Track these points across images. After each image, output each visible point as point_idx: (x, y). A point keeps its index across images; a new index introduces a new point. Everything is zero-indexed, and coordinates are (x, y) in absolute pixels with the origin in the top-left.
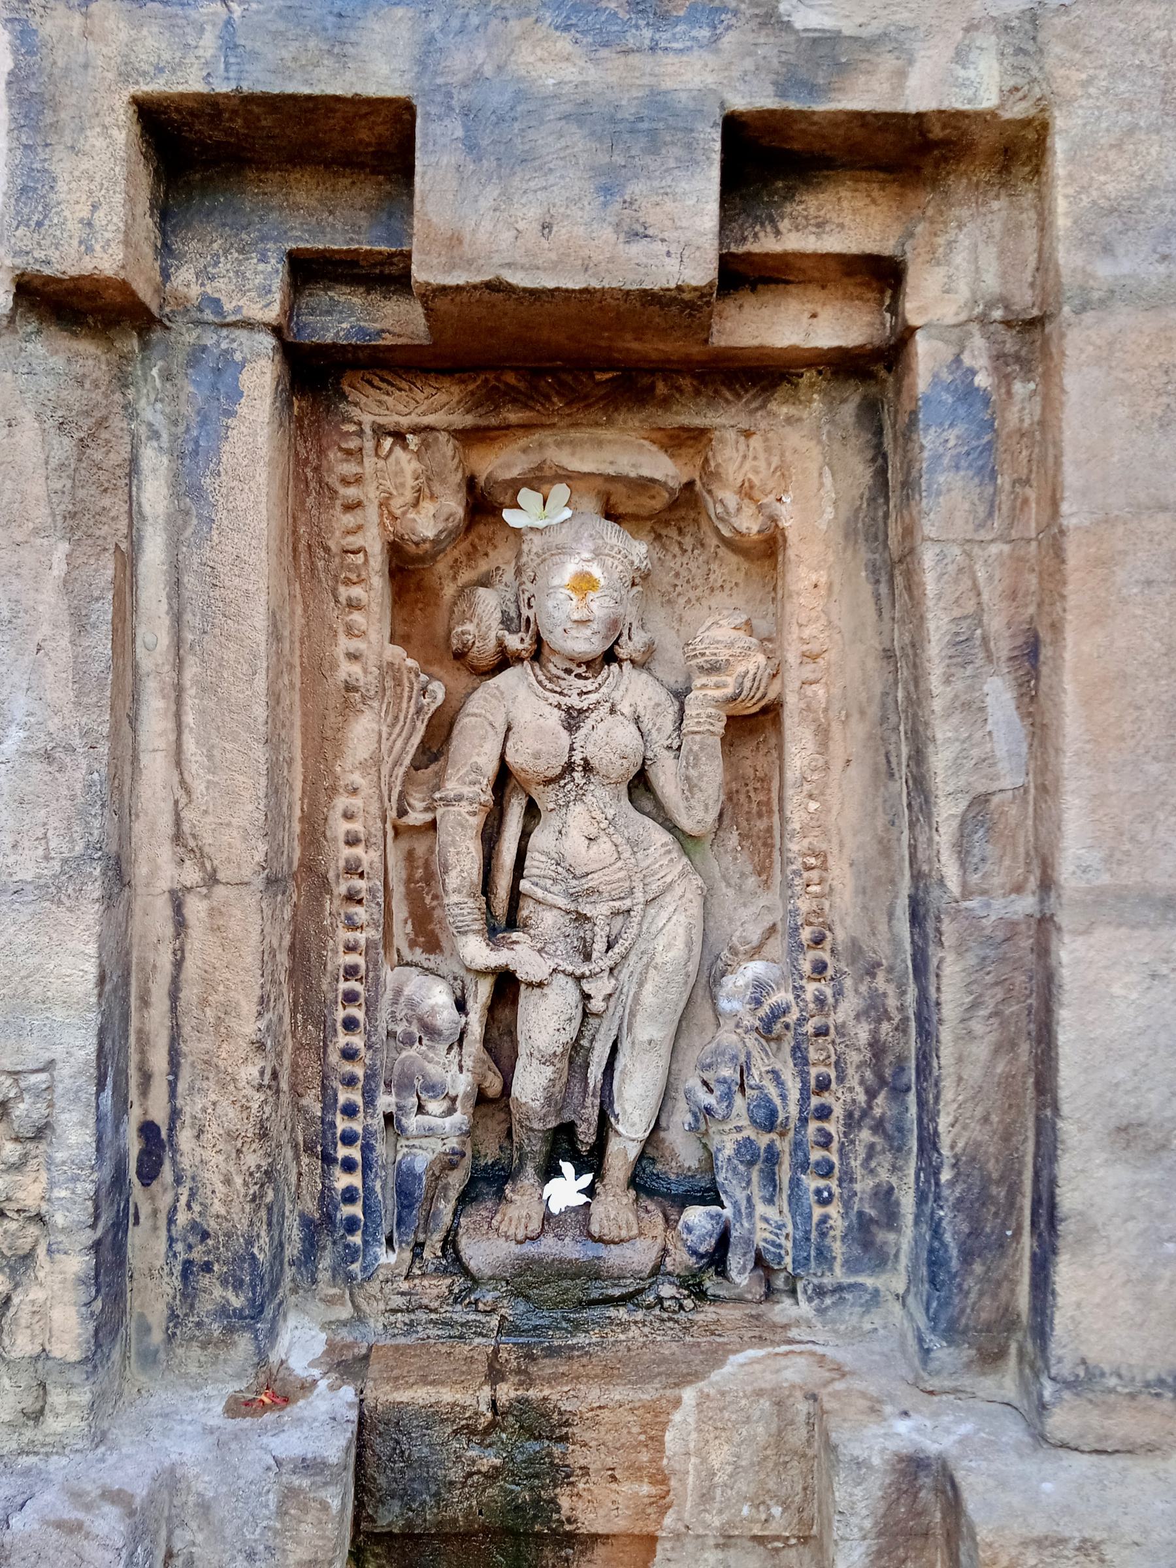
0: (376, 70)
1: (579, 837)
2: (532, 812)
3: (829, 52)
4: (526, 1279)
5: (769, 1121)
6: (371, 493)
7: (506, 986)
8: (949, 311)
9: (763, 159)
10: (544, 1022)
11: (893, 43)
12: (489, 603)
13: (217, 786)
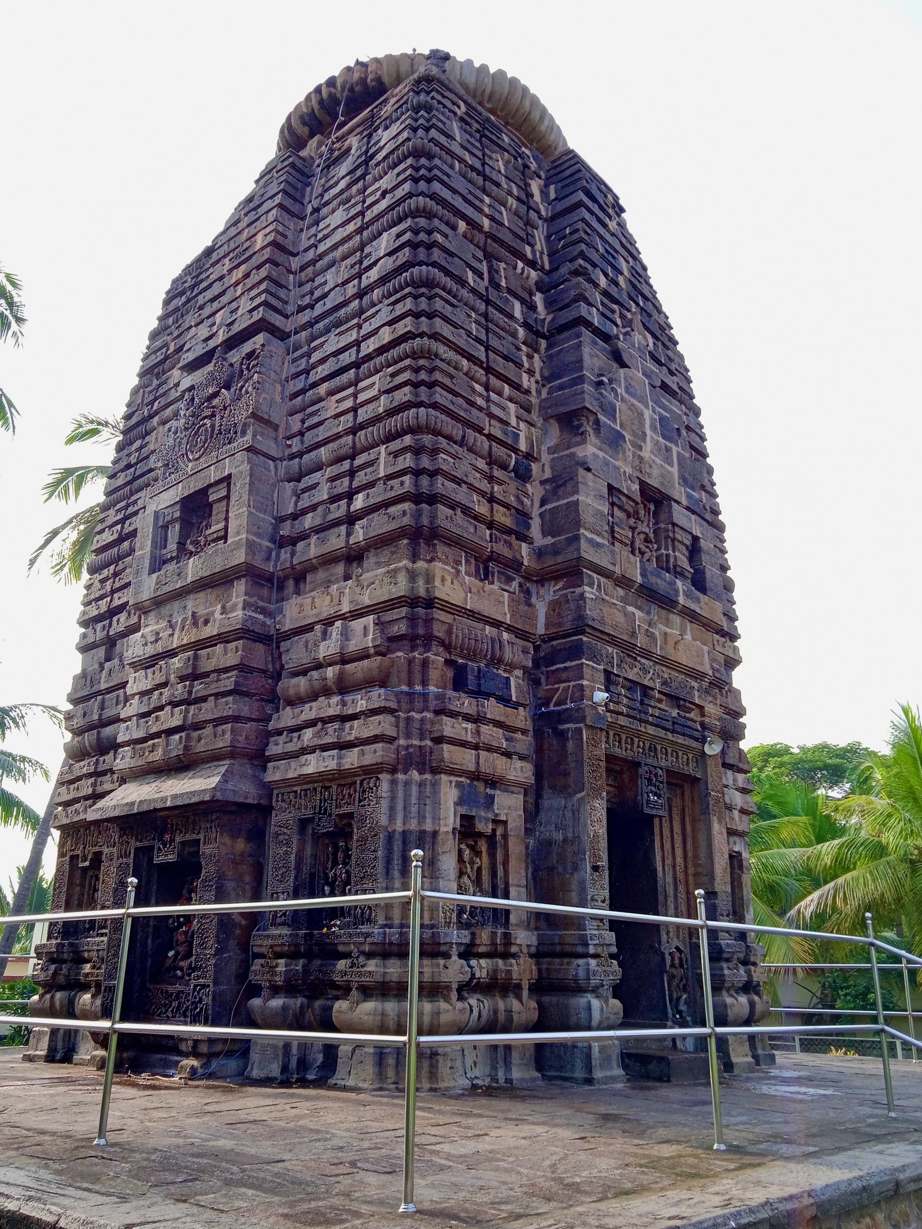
3: (497, 815)
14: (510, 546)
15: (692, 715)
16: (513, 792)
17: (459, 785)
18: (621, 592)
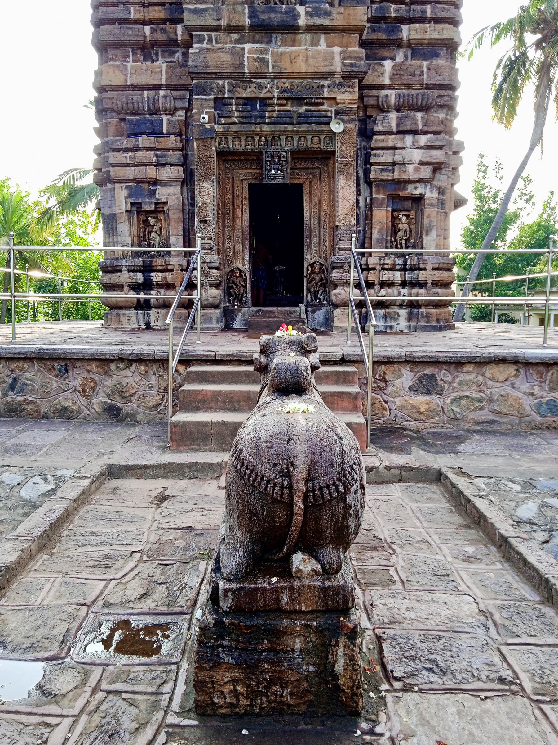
0: (140, 201)
3: (158, 199)
13: (135, 232)
14: (164, 31)
15: (325, 107)
17: (127, 187)
18: (235, 36)
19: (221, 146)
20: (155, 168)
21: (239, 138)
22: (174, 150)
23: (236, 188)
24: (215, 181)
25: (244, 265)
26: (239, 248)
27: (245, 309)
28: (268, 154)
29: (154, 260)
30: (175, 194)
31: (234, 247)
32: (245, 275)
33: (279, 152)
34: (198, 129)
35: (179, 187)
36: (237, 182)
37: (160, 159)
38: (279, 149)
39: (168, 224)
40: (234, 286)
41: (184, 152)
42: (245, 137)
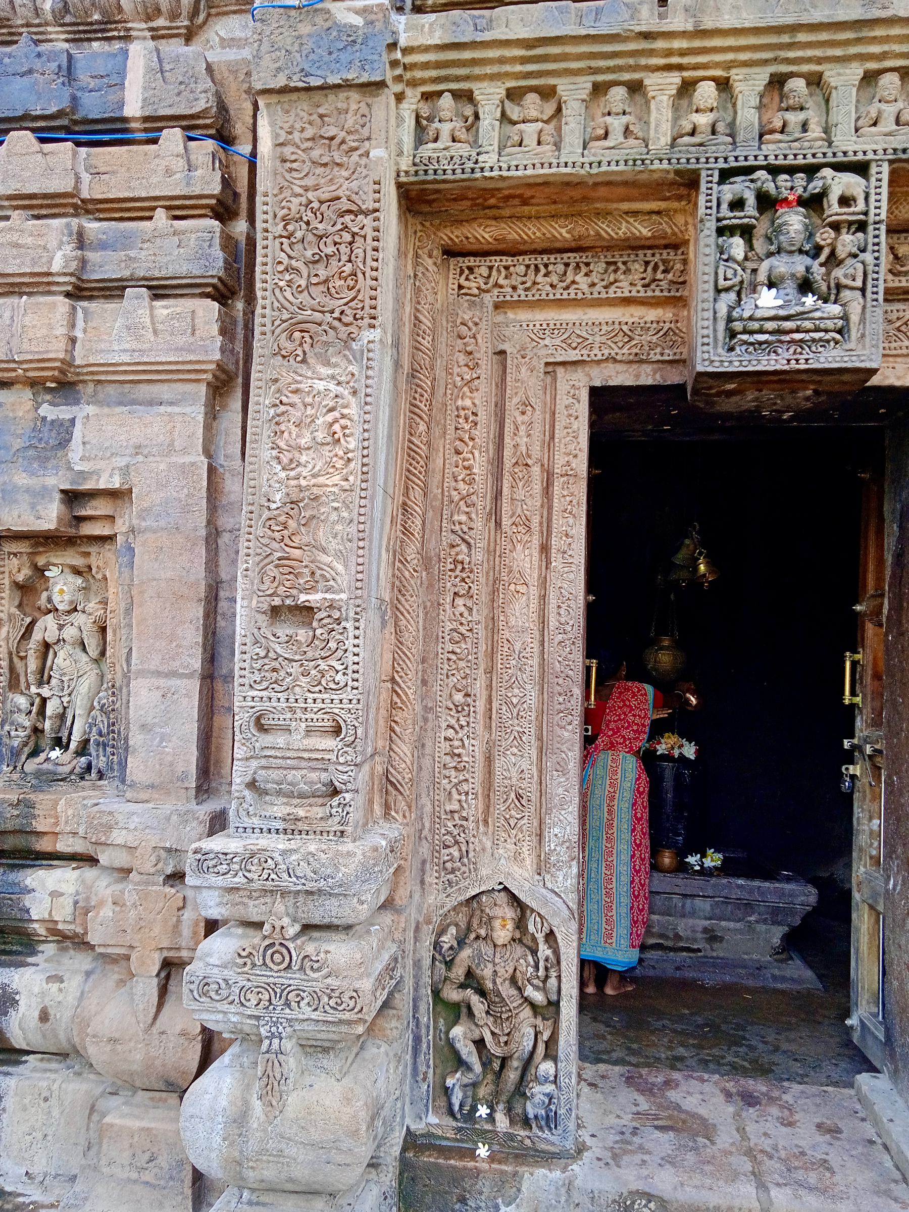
1: (61, 660)
2: (55, 653)
3: (83, 475)
4: (38, 774)
5: (100, 734)
6: (6, 569)
7: (44, 701)
8: (124, 529)
9: (72, 497)
10: (51, 708)
11: (97, 473)
12: (44, 595)
16: (152, 403)
19: (428, 150)
20: (62, 304)
21: (547, 93)
22: (180, 208)
23: (512, 414)
24: (384, 363)
25: (542, 867)
26: (516, 765)
27: (539, 1180)
28: (739, 187)
29: (42, 799)
30: (171, 448)
31: (489, 760)
32: (550, 936)
33: (811, 170)
34: (286, 39)
35: (197, 412)
36: (526, 380)
37: (93, 256)
38: (811, 147)
39: (128, 611)
40: (478, 1005)
41: (240, 227)
42: (585, 84)
